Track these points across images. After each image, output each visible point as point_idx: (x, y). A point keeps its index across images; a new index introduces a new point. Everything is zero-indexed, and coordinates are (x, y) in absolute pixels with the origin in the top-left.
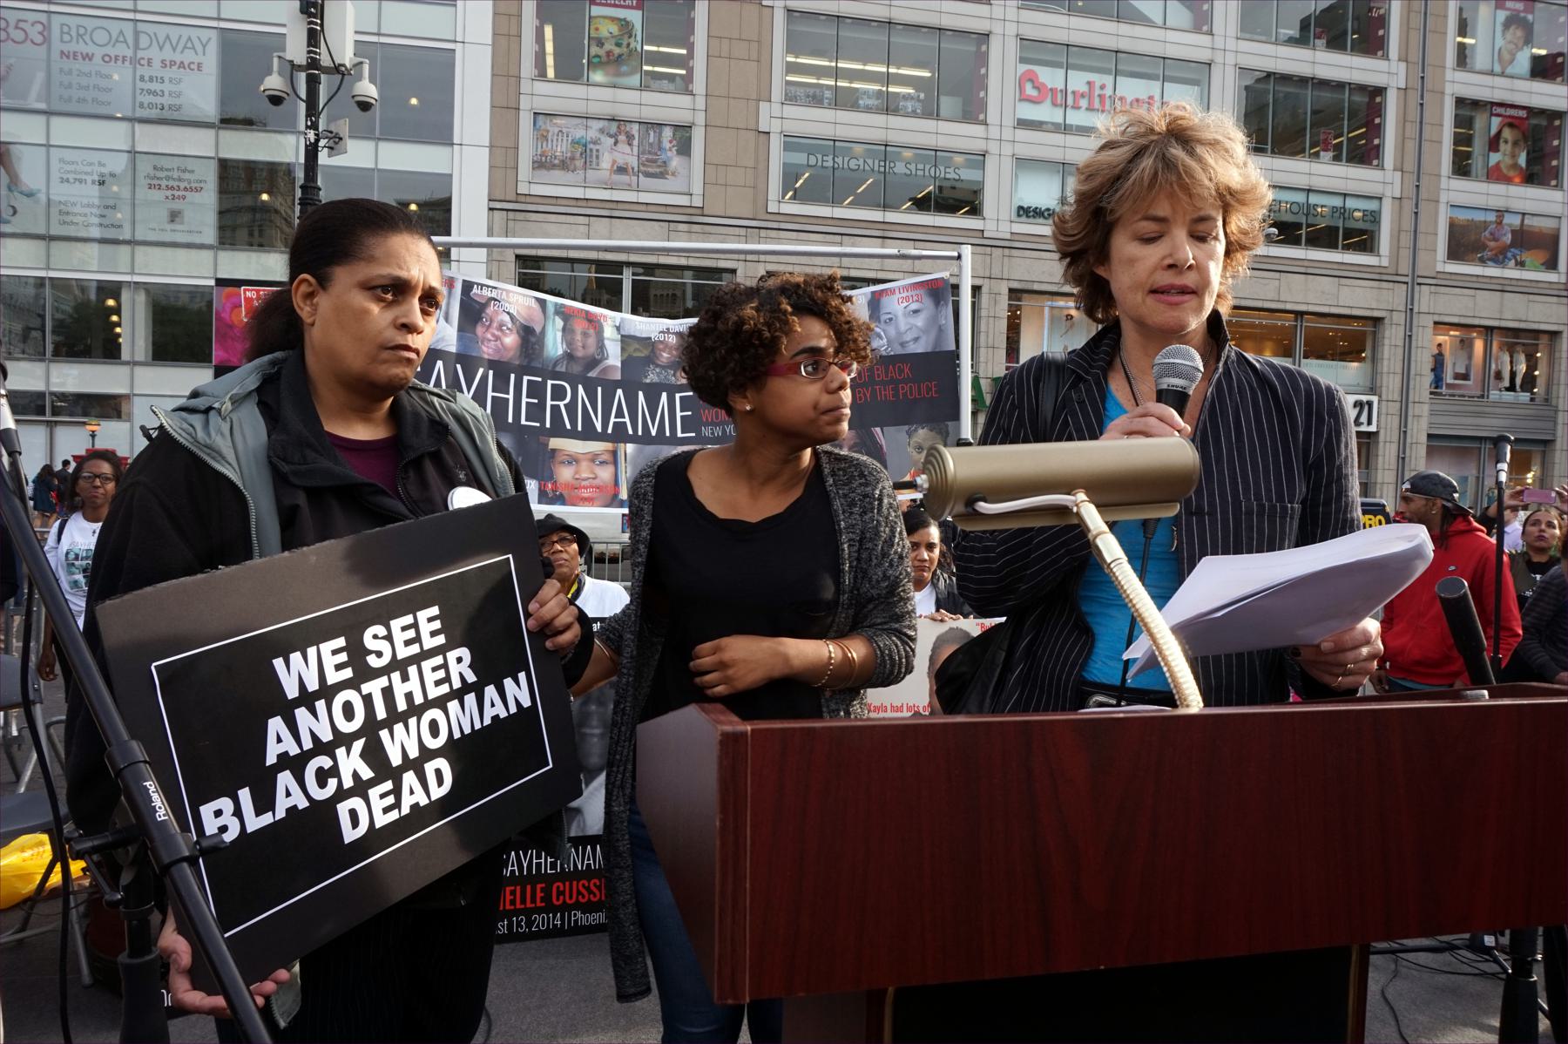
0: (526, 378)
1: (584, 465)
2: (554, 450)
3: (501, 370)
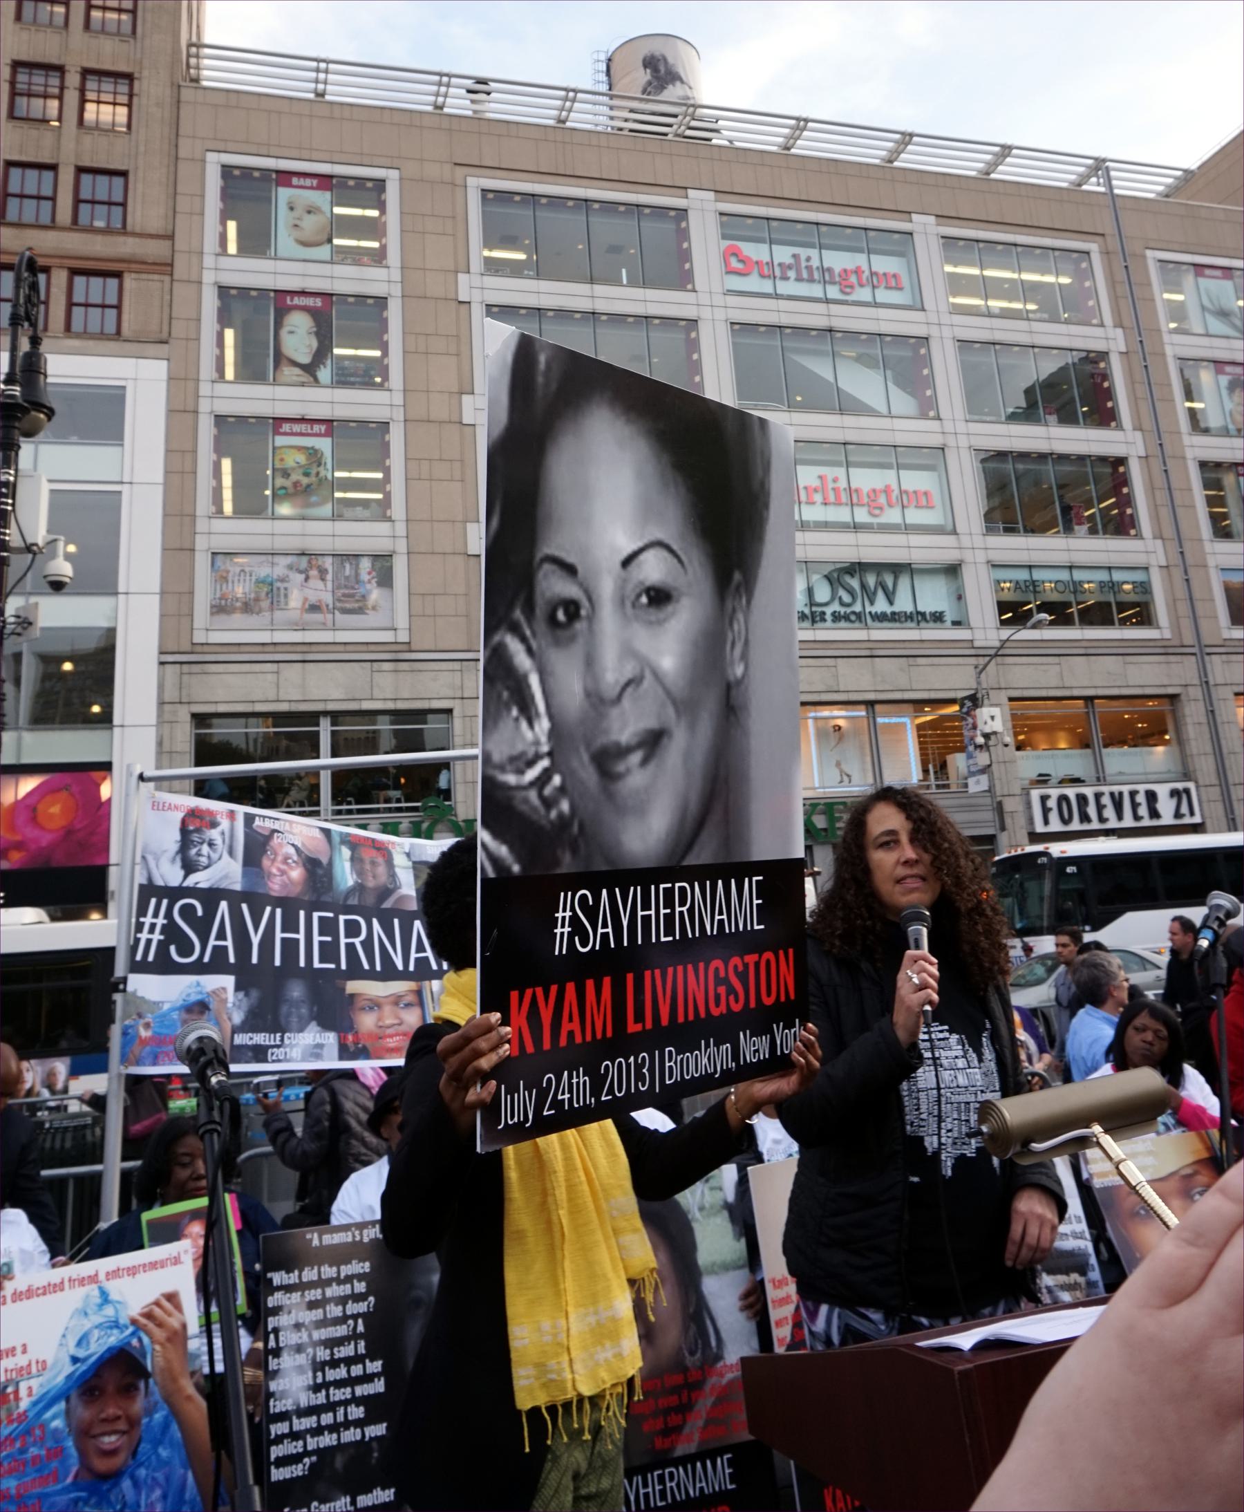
0: (316, 915)
1: (387, 1009)
2: (352, 996)
3: (289, 906)
